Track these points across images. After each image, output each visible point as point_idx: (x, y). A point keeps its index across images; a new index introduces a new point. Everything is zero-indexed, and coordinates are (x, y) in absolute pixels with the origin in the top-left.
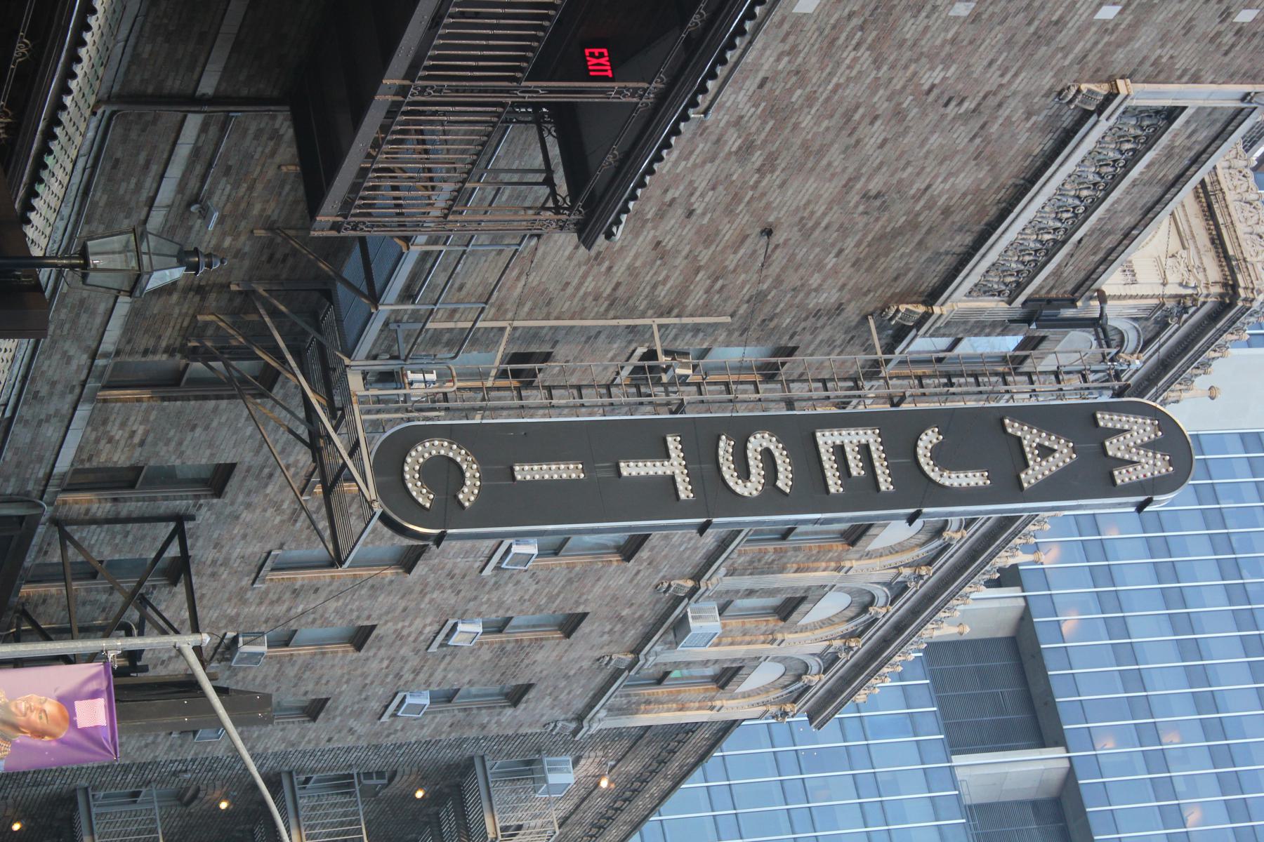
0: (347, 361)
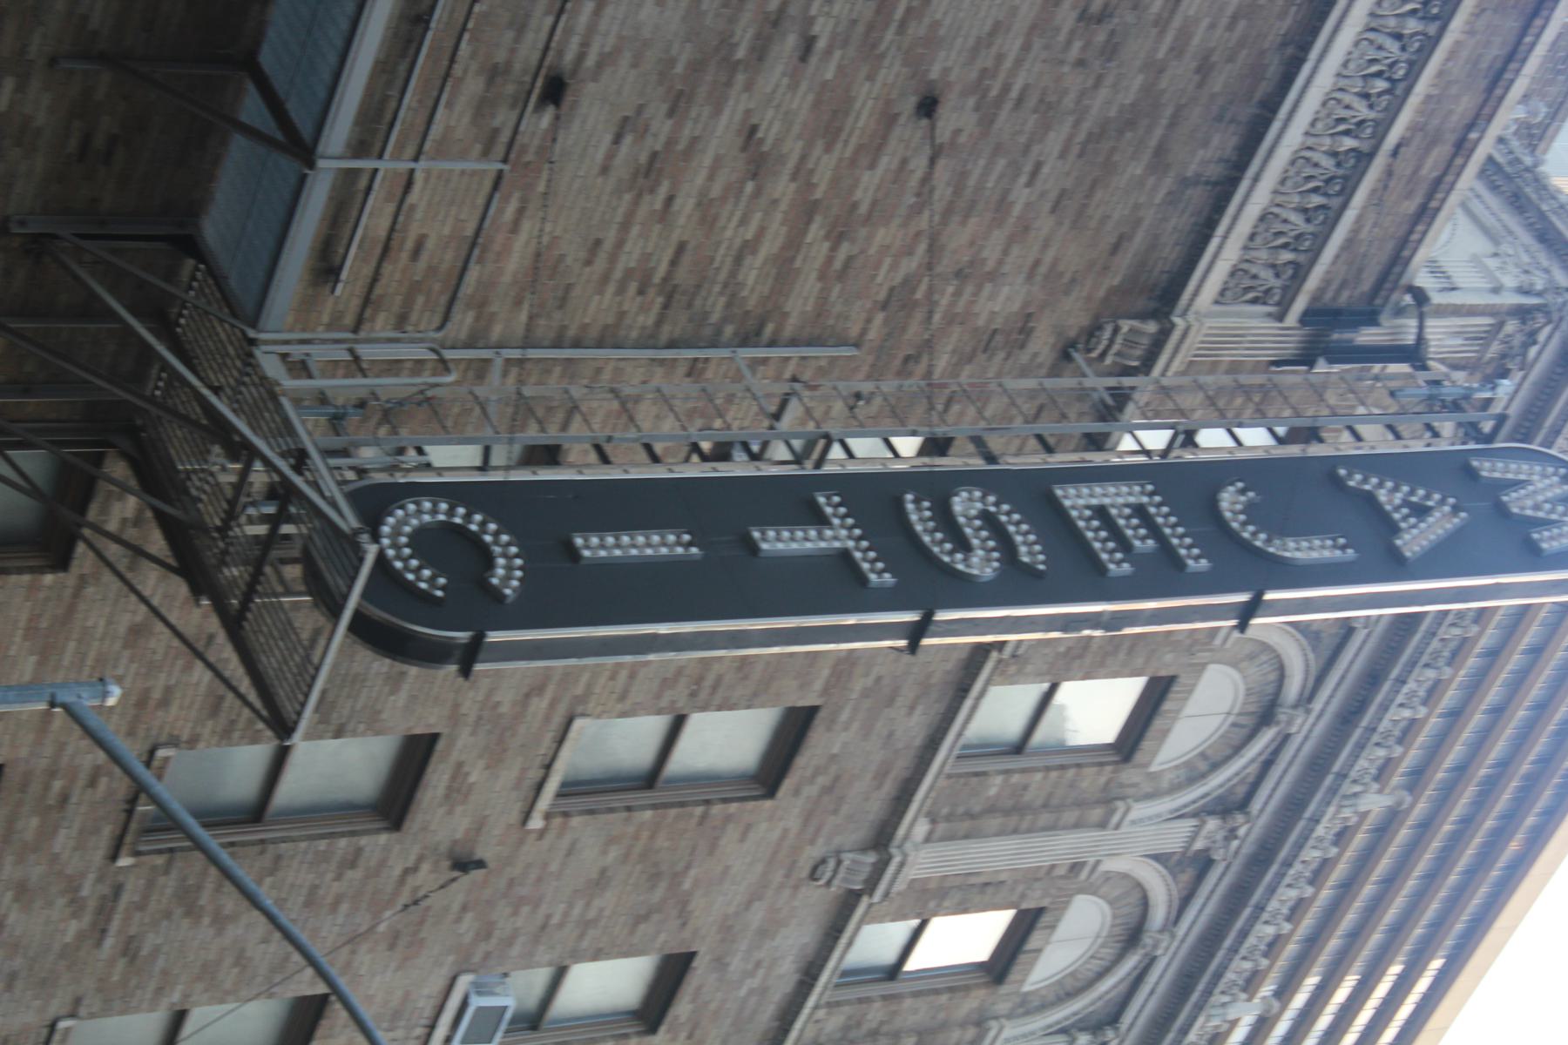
0: (252, 334)
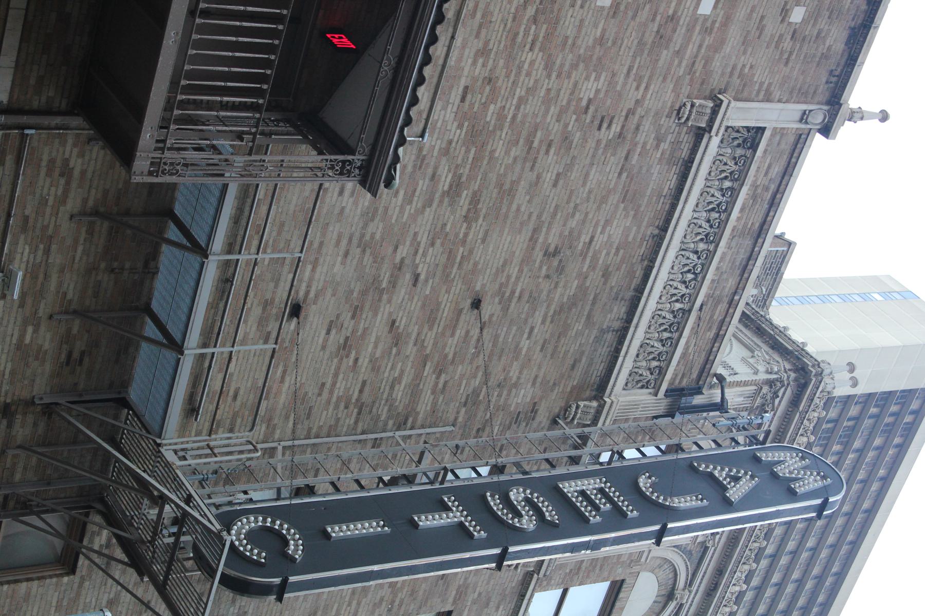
0: (158, 441)
